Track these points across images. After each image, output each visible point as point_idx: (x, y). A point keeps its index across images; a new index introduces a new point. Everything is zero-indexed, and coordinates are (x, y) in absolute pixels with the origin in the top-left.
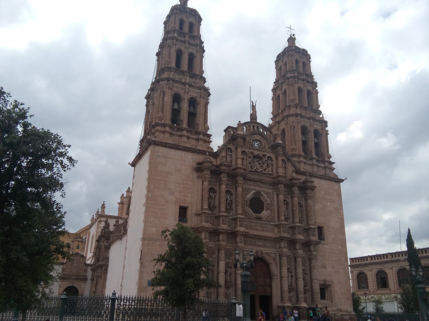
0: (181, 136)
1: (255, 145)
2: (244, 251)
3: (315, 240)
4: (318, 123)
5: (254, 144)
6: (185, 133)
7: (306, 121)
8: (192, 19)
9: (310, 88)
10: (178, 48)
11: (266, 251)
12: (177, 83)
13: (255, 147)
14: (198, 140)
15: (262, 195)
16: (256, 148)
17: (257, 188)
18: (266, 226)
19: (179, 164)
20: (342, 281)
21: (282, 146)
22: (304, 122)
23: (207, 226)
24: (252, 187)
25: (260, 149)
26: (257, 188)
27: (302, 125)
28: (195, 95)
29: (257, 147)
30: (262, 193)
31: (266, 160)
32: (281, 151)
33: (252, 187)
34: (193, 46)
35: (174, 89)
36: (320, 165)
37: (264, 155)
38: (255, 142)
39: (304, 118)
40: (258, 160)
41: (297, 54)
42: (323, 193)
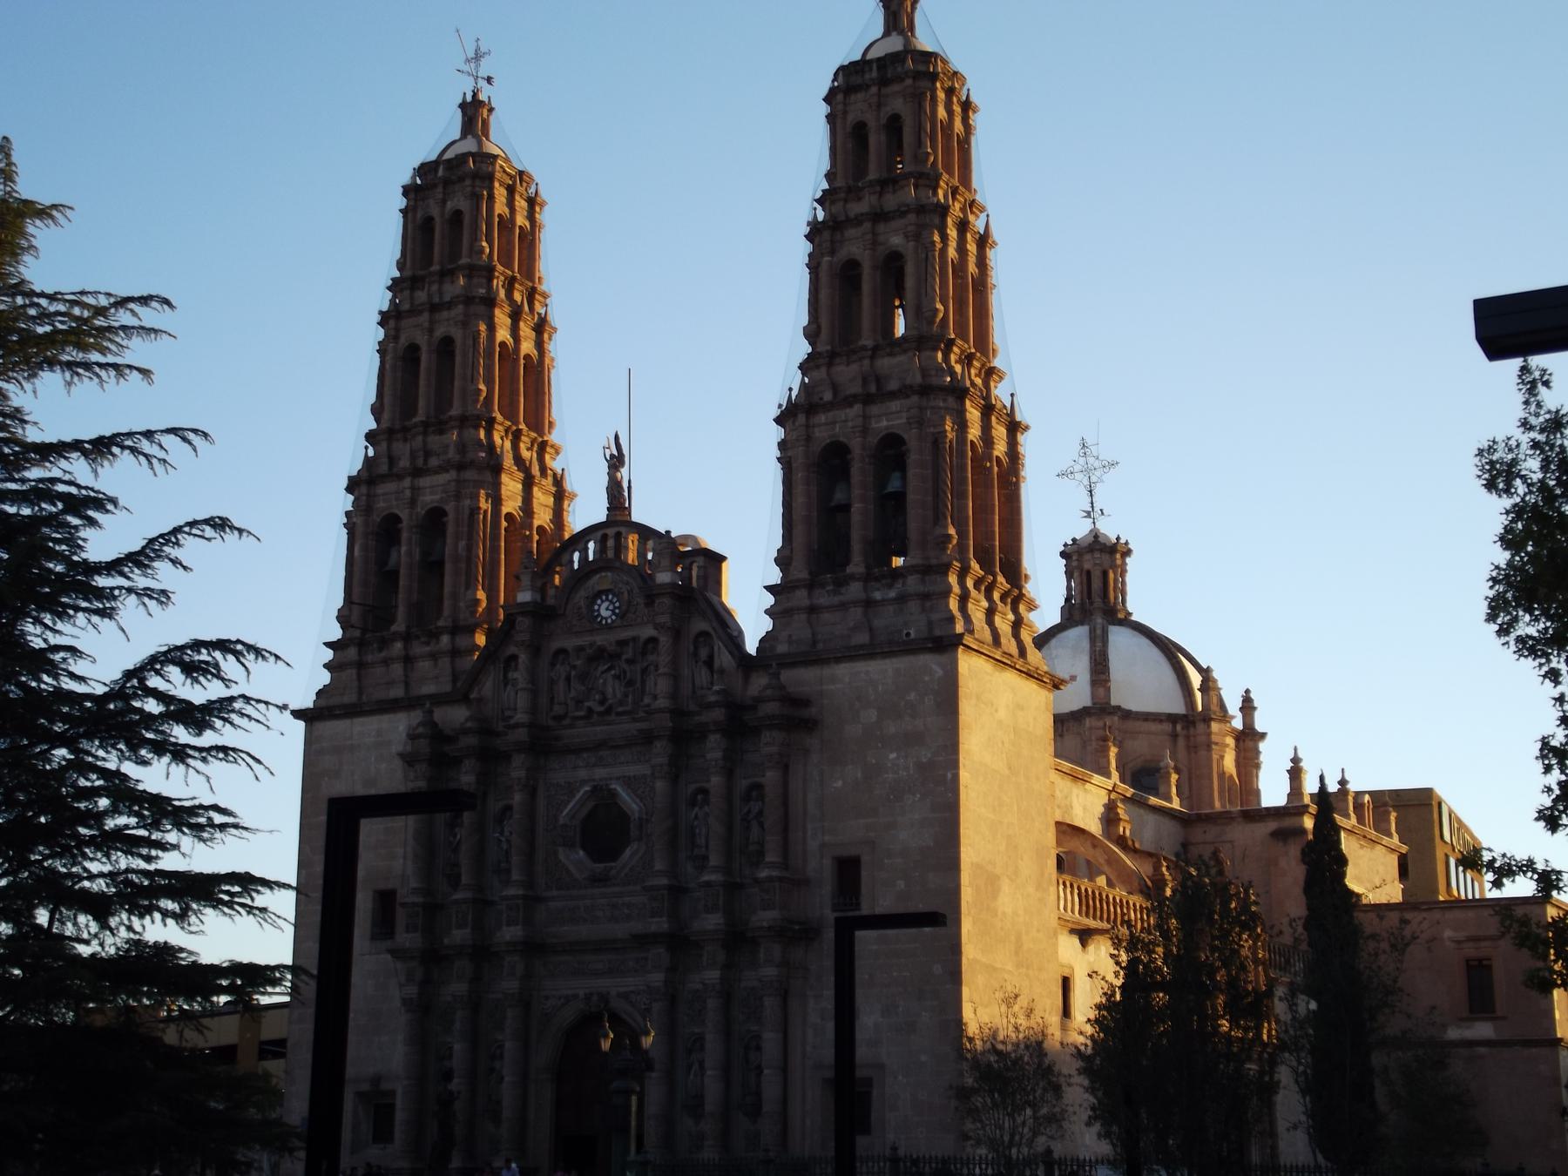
0: (386, 662)
1: (599, 615)
2: (547, 998)
3: (765, 924)
4: (895, 405)
5: (598, 610)
6: (399, 645)
7: (843, 418)
8: (456, 199)
9: (896, 241)
10: (407, 344)
11: (622, 990)
12: (383, 482)
13: (599, 619)
14: (434, 656)
15: (613, 794)
16: (604, 622)
17: (600, 773)
18: (627, 899)
19: (373, 759)
20: (923, 1058)
21: (663, 594)
22: (834, 423)
23: (407, 945)
24: (582, 774)
25: (615, 625)
26: (600, 773)
27: (823, 444)
28: (437, 497)
29: (606, 619)
30: (613, 786)
31: (630, 662)
32: (663, 614)
33: (582, 774)
34: (449, 308)
35: (378, 506)
36: (878, 595)
37: (622, 643)
38: (603, 602)
39: (829, 411)
40: (606, 667)
41: (860, 96)
42: (871, 715)
